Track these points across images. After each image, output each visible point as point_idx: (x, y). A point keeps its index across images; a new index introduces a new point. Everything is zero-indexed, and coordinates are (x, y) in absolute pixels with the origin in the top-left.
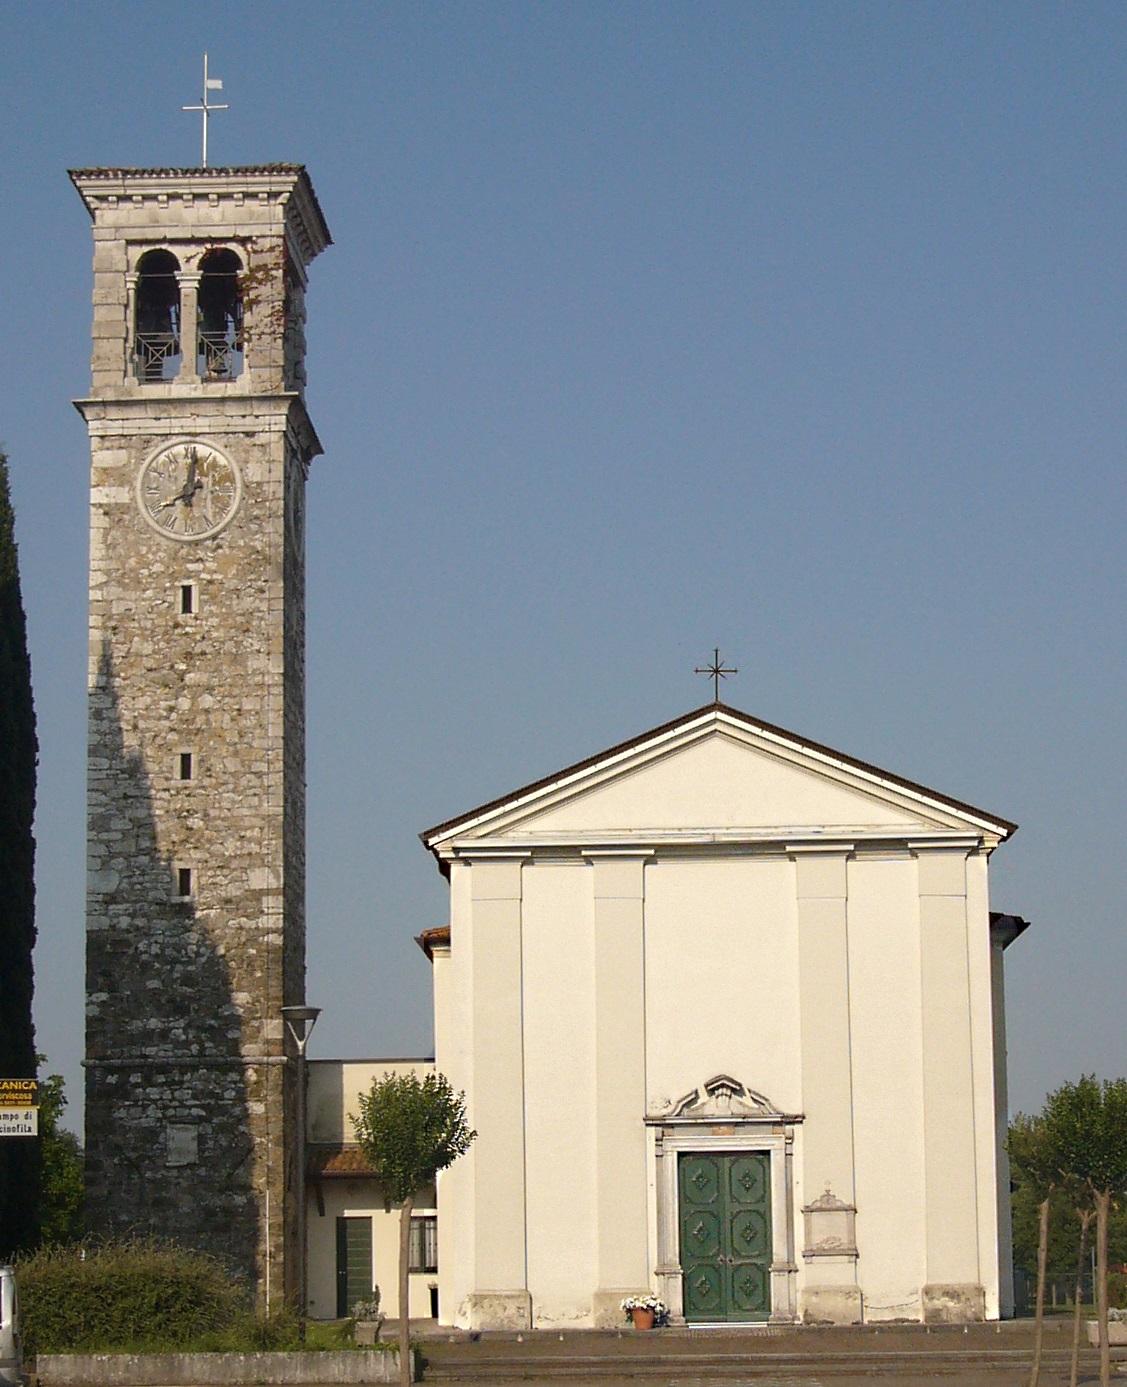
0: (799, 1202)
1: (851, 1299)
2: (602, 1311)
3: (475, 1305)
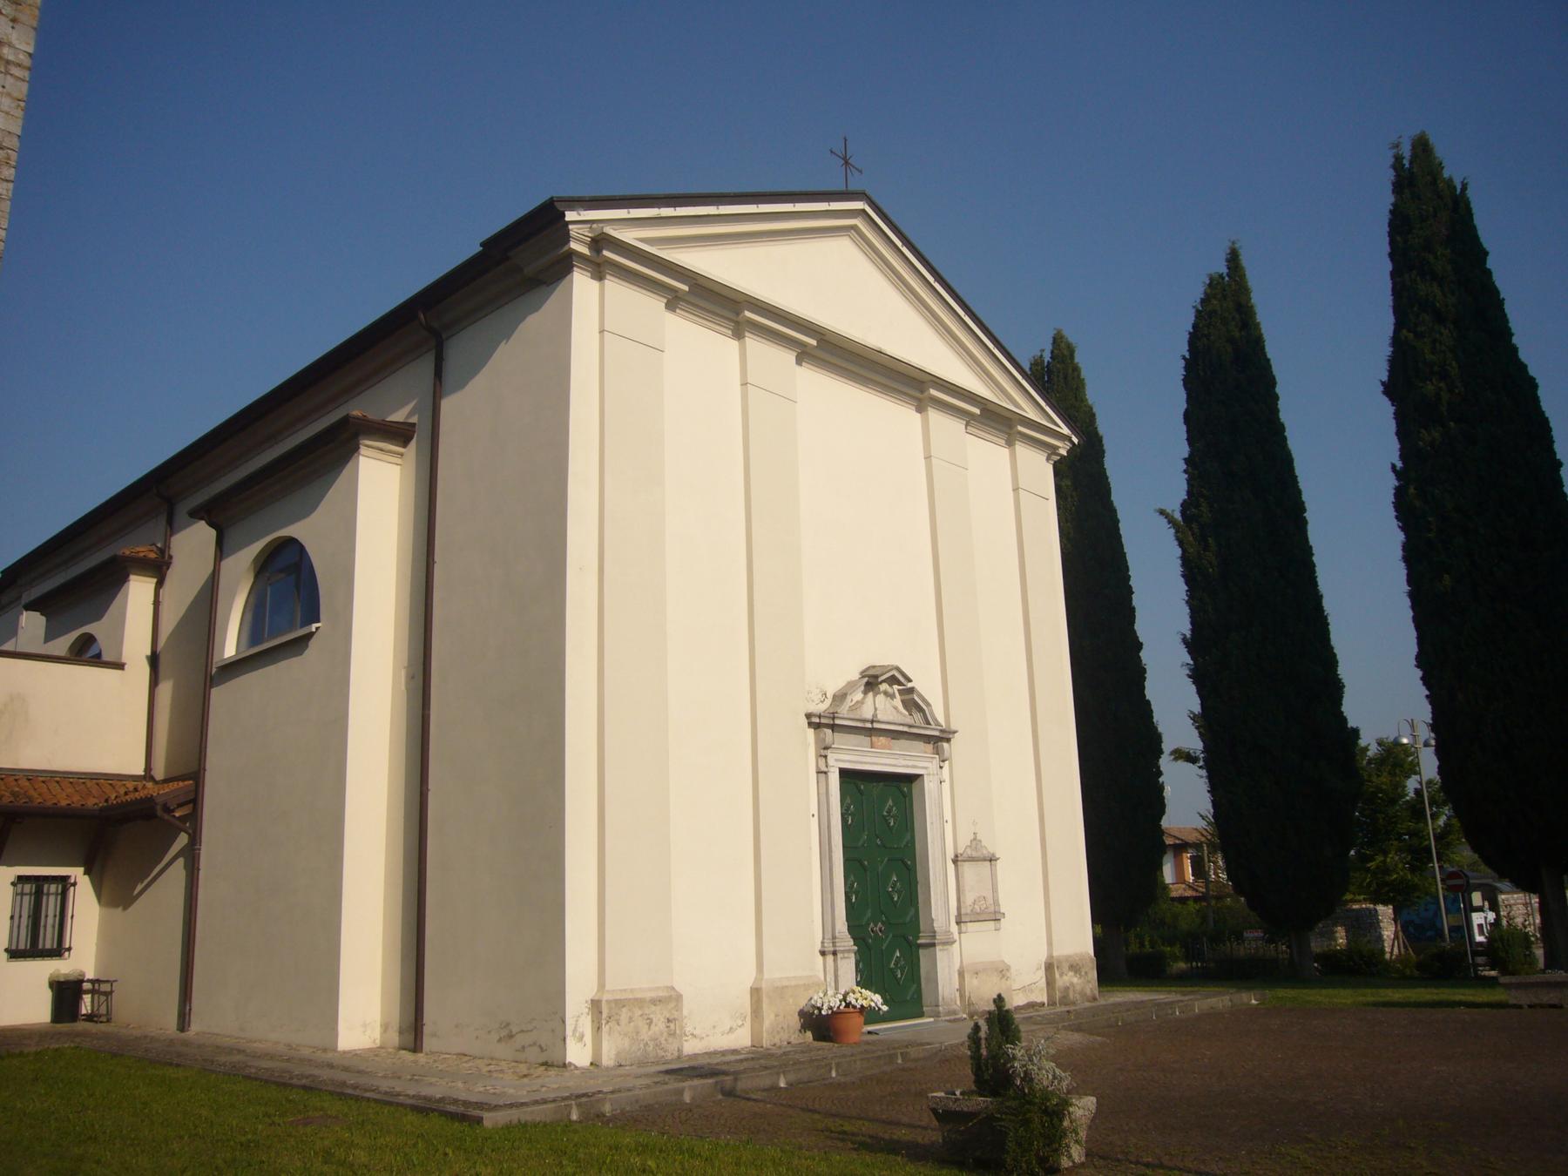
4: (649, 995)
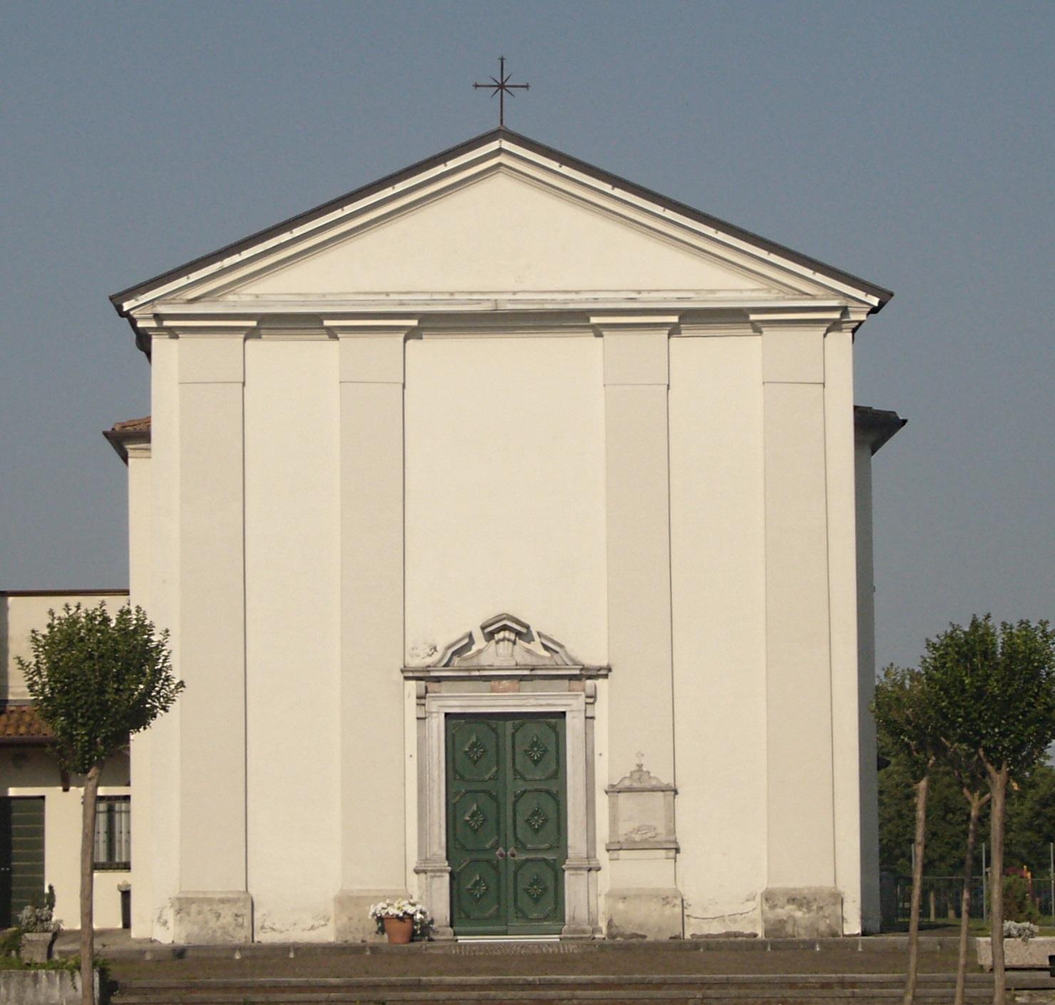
0: (603, 778)
1: (668, 906)
2: (345, 919)
3: (179, 911)
4: (218, 896)
